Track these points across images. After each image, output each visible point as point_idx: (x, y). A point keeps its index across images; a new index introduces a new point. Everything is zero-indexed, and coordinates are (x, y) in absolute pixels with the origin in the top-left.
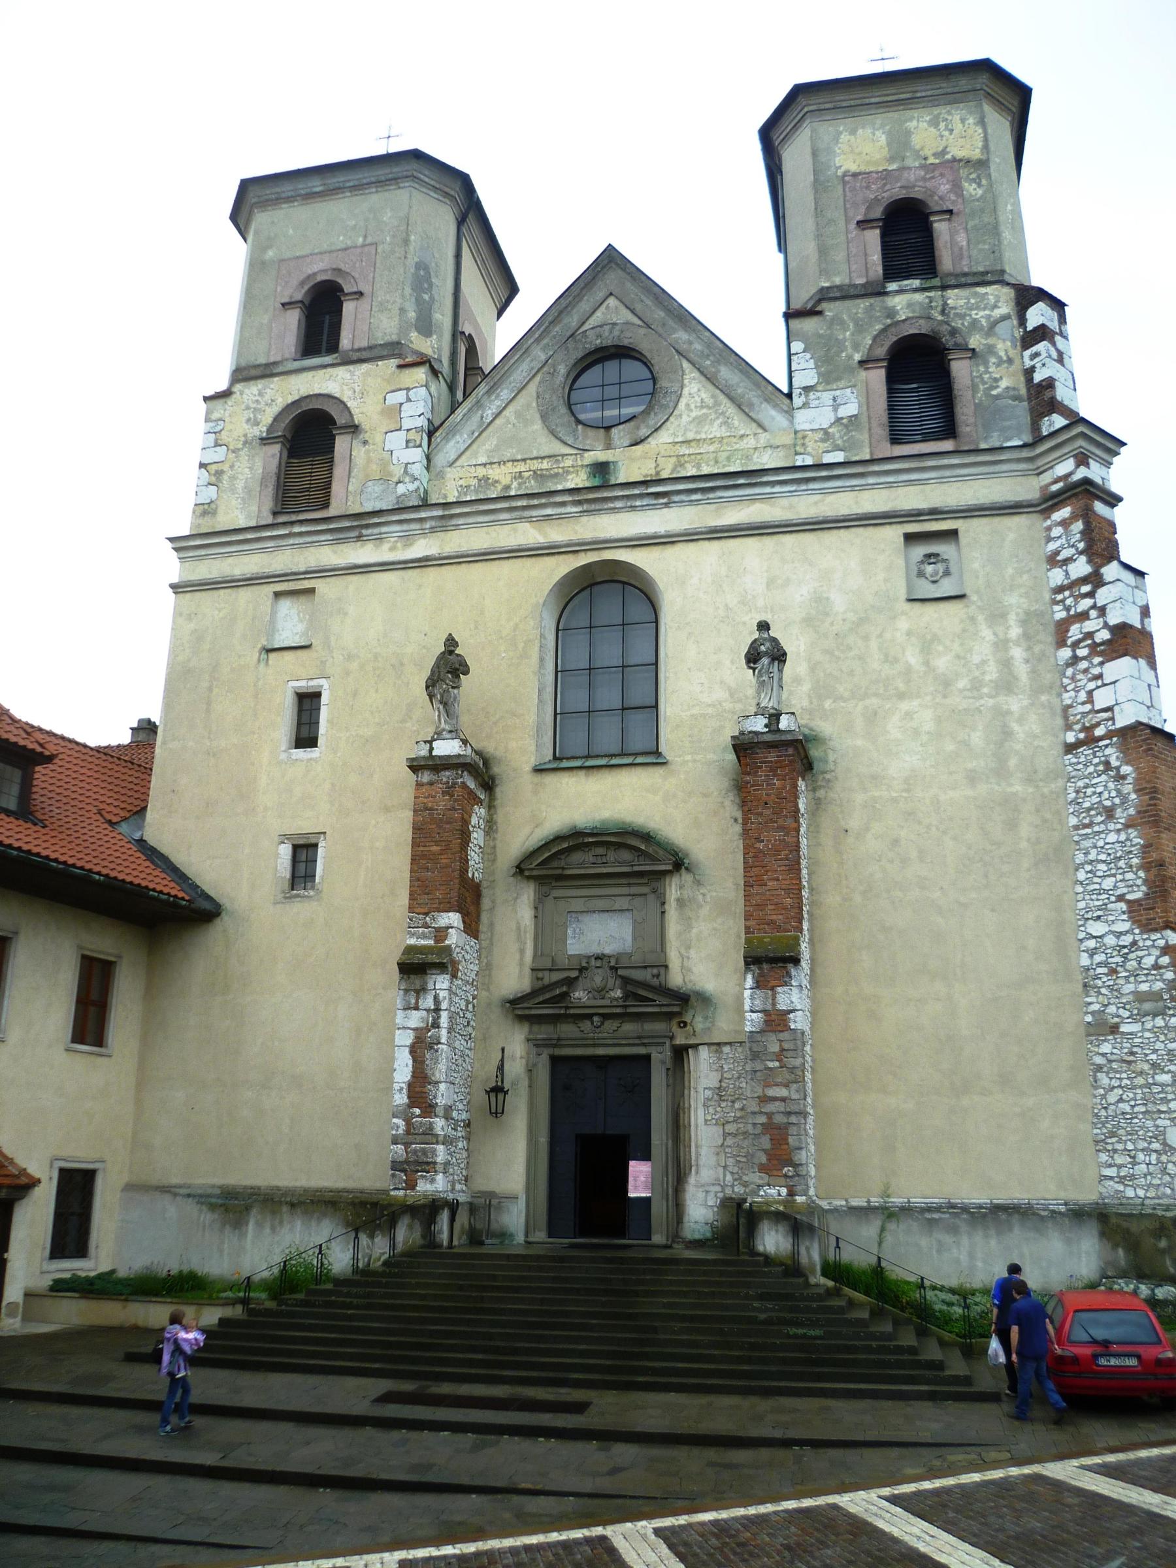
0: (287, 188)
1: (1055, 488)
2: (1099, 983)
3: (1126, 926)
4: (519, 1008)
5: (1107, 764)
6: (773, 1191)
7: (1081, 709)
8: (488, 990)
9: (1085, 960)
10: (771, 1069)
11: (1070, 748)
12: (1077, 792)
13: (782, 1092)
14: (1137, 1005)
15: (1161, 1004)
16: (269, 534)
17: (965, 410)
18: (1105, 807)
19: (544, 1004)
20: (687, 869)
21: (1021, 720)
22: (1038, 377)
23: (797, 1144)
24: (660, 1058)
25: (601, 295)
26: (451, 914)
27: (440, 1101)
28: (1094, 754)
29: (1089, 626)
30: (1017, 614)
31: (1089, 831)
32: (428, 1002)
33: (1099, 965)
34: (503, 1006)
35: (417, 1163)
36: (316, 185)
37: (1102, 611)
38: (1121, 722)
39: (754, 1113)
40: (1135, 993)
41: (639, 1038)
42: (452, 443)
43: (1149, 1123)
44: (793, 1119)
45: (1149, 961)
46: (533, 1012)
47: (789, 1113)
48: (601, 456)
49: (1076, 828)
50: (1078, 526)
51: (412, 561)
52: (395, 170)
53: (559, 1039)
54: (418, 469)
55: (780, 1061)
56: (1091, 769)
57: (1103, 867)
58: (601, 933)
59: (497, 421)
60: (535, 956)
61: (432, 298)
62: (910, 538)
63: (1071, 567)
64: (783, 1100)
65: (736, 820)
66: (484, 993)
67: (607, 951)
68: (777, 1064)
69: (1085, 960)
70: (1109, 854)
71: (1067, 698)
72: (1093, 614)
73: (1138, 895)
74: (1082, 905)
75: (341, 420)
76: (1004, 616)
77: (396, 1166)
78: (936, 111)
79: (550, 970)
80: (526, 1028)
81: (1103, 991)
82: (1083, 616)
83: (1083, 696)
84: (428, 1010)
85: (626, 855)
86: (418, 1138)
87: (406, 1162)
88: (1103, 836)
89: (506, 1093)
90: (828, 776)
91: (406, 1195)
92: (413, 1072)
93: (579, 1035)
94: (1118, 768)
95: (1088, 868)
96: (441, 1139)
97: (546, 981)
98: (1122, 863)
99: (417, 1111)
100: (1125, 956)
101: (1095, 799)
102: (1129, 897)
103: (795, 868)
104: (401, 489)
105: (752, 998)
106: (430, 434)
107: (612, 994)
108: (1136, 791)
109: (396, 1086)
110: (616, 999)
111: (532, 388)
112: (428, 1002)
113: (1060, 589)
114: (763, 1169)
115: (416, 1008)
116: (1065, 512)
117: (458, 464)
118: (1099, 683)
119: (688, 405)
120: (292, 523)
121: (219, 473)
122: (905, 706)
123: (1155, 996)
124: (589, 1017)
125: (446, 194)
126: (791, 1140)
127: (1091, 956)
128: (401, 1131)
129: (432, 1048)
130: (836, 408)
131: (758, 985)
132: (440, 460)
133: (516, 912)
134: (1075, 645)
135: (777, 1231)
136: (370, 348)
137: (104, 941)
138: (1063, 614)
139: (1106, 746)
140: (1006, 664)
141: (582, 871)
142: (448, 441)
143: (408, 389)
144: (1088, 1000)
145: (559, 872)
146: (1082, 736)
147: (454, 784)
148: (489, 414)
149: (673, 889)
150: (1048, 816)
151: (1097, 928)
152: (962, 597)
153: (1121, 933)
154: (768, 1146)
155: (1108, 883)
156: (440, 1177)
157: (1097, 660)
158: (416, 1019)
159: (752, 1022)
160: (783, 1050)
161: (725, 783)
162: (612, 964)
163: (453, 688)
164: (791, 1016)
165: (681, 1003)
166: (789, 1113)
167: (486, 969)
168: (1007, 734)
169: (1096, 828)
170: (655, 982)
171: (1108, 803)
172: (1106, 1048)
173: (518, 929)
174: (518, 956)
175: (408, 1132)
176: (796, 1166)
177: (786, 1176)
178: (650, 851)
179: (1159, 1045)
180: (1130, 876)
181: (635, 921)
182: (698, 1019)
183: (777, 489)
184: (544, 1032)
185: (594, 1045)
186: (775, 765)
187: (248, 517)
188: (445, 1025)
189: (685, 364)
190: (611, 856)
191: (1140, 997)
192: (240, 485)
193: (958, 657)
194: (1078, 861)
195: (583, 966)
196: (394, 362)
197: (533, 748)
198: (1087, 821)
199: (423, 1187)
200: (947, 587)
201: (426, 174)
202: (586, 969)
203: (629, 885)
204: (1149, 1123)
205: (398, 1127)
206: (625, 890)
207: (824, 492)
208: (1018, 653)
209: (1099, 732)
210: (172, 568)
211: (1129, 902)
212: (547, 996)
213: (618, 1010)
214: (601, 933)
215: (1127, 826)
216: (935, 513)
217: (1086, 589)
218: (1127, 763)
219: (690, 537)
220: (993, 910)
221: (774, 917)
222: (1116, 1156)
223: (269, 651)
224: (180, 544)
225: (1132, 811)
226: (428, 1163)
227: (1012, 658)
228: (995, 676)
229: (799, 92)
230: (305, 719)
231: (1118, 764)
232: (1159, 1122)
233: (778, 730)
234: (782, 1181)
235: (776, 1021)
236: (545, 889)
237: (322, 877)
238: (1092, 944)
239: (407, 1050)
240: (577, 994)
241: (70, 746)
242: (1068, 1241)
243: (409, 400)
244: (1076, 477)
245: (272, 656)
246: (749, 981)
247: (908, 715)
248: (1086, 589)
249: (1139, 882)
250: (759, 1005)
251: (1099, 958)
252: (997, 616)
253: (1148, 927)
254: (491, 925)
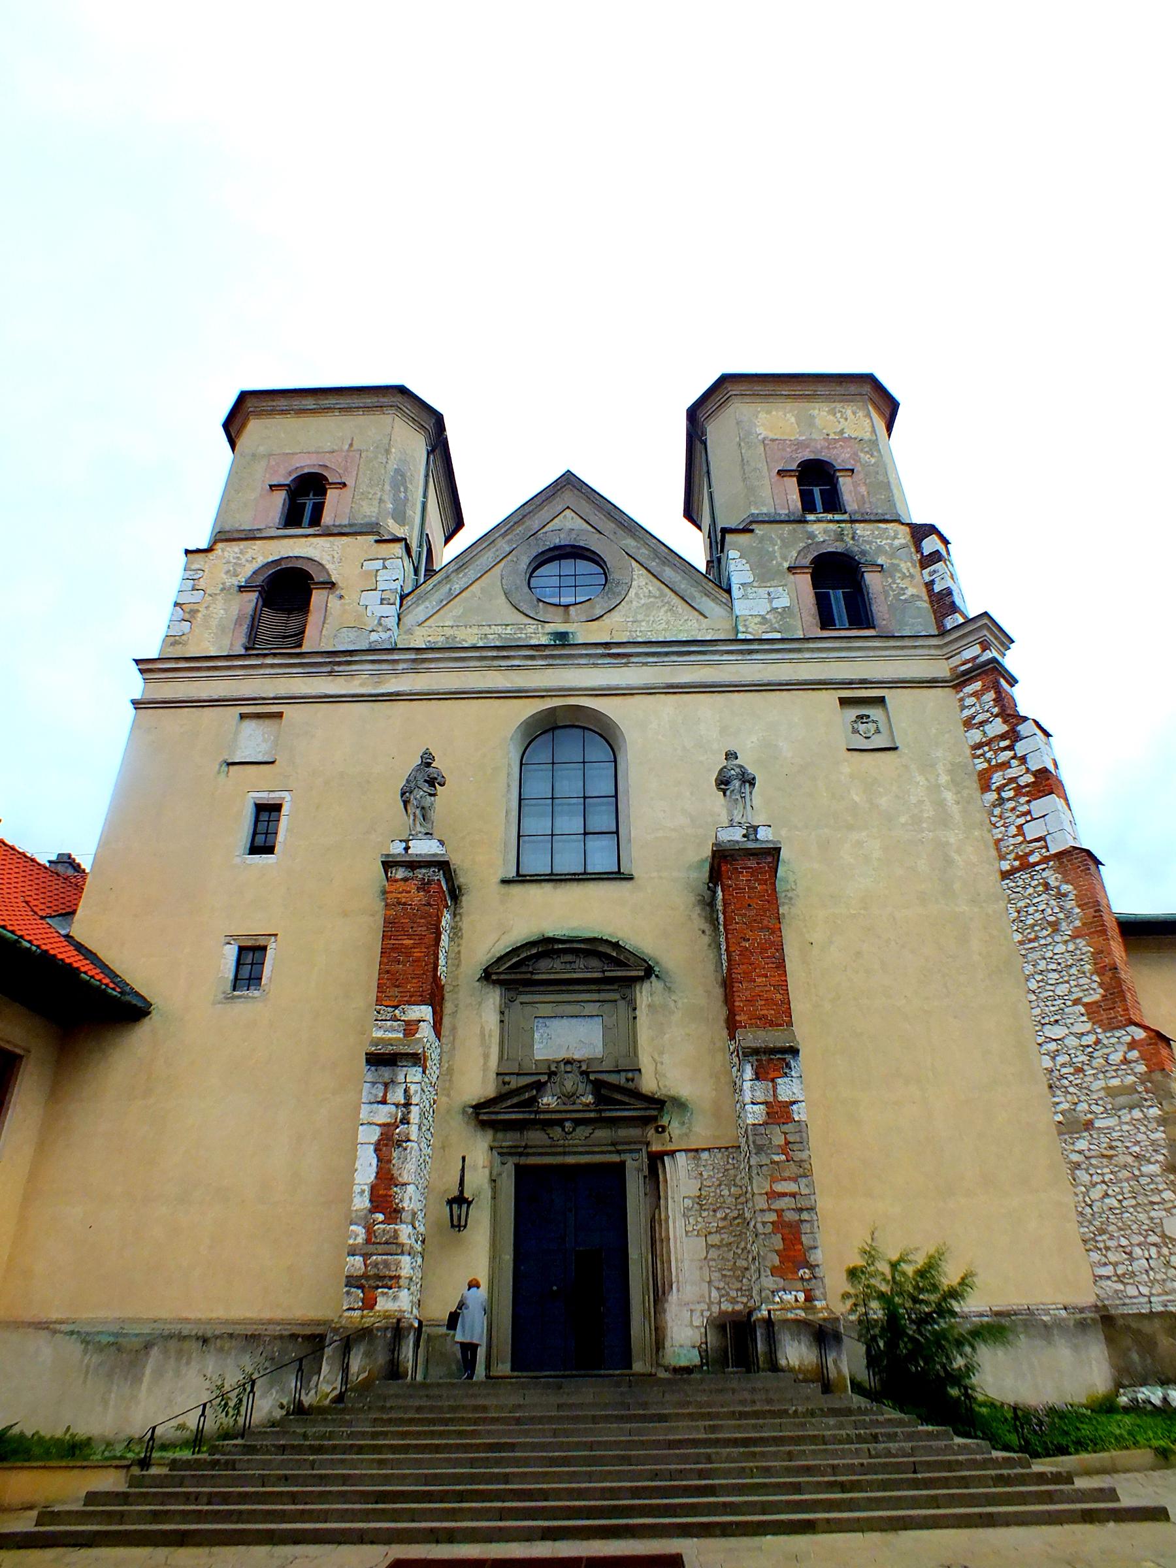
0: (282, 403)
1: (963, 668)
2: (1066, 1082)
3: (1088, 1026)
4: (483, 1115)
5: (1047, 886)
6: (789, 1297)
7: (1012, 841)
8: (448, 1096)
9: (1047, 1062)
10: (777, 1163)
11: (1005, 875)
12: (1019, 912)
13: (791, 1187)
14: (1109, 1099)
15: (1136, 1096)
16: (241, 663)
17: (881, 609)
18: (1049, 923)
19: (507, 1112)
20: (657, 976)
21: (959, 851)
22: (937, 588)
23: (812, 1244)
24: (634, 1167)
25: (560, 508)
26: (423, 1007)
28: (1032, 878)
29: (1011, 773)
30: (944, 765)
31: (1036, 944)
32: (398, 1096)
33: (1063, 1065)
34: (464, 1112)
35: (379, 1277)
36: (309, 403)
37: (1023, 760)
38: (1053, 851)
39: (762, 1211)
40: (1107, 1089)
41: (613, 1144)
42: (421, 608)
43: (1142, 1217)
44: (805, 1216)
45: (1116, 1057)
46: (501, 1117)
47: (801, 1210)
48: (562, 628)
49: (1021, 943)
50: (992, 695)
51: (383, 695)
52: (382, 400)
53: (526, 1147)
54: (392, 622)
55: (786, 1154)
56: (1031, 890)
57: (1055, 975)
58: (569, 1036)
59: (463, 594)
60: (501, 1058)
61: (406, 498)
62: (844, 702)
63: (987, 728)
64: (793, 1195)
65: (703, 932)
66: (444, 1099)
67: (576, 1057)
68: (783, 1157)
69: (1047, 1062)
70: (1059, 964)
71: (997, 834)
72: (1014, 763)
73: (1097, 997)
74: (1037, 1011)
75: (319, 577)
76: (933, 766)
77: (352, 1282)
78: (833, 405)
79: (518, 1074)
80: (489, 1135)
81: (1071, 1090)
82: (1006, 765)
83: (1013, 830)
84: (397, 1105)
85: (594, 963)
86: (380, 1248)
87: (365, 1276)
88: (1050, 948)
89: (469, 1203)
90: (789, 894)
91: (362, 1317)
92: (377, 1173)
93: (549, 1142)
94: (1058, 888)
95: (1039, 978)
96: (407, 1248)
97: (513, 1085)
98: (1074, 971)
99: (380, 1217)
100: (1090, 1055)
101: (1038, 916)
102: (1086, 1000)
103: (781, 965)
104: (374, 637)
105: (752, 1089)
106: (403, 598)
107: (583, 1099)
108: (1079, 906)
109: (357, 1189)
110: (587, 1105)
111: (497, 570)
112: (398, 1096)
113: (979, 746)
114: (774, 1271)
115: (384, 1102)
116: (977, 686)
117: (426, 624)
118: (1029, 818)
119: (637, 594)
120: (265, 655)
121: (194, 612)
122: (854, 836)
123: (1132, 1090)
124: (560, 1123)
126: (804, 1239)
127: (1053, 1058)
128: (360, 1240)
129: (399, 1146)
130: (771, 601)
131: (757, 1077)
132: (408, 620)
133: (481, 1017)
134: (999, 790)
135: (799, 1342)
136: (351, 525)
138: (986, 765)
139: (1043, 870)
140: (940, 804)
141: (552, 977)
142: (418, 605)
143: (384, 559)
144: (1057, 1100)
145: (529, 976)
146: (1017, 863)
147: (429, 882)
148: (457, 588)
149: (644, 995)
150: (995, 933)
151: (1058, 1032)
153: (1083, 1034)
154: (780, 1245)
155: (1062, 990)
156: (404, 1294)
157: (1023, 800)
158: (384, 1114)
159: (755, 1114)
160: (787, 1143)
161: (692, 899)
162: (584, 1068)
163: (431, 795)
164: (795, 1107)
165: (655, 1109)
166: (801, 1210)
167: (448, 1074)
168: (949, 862)
169: (1043, 942)
170: (631, 1085)
171: (1052, 919)
172: (1082, 1145)
173: (482, 1034)
174: (482, 1061)
175: (368, 1241)
176: (812, 1267)
177: (802, 1278)
178: (622, 958)
179: (1140, 1137)
180: (1082, 981)
181: (605, 1028)
182: (675, 1124)
183: (725, 657)
184: (509, 1139)
185: (565, 1154)
186: (741, 880)
187: (220, 648)
188: (417, 1121)
189: (634, 564)
190: (581, 963)
191: (1111, 1092)
192: (214, 623)
193: (897, 797)
194: (1027, 973)
195: (552, 1072)
197: (501, 862)
198: (1032, 936)
199: (384, 1304)
200: (879, 741)
201: (408, 407)
202: (555, 1073)
203: (599, 991)
204: (1142, 1217)
205: (357, 1235)
206: (595, 996)
207: (763, 662)
208: (949, 796)
209: (1033, 859)
210: (136, 686)
211: (1085, 1005)
212: (515, 1100)
213: (592, 1115)
214: (569, 1036)
215: (1073, 938)
216: (864, 683)
217: (1003, 744)
218: (1067, 883)
219: (649, 691)
220: (955, 1017)
221: (765, 1012)
222: (1109, 1254)
224: (145, 666)
225: (1078, 923)
226: (391, 1278)
227: (945, 799)
228: (932, 813)
229: (693, 414)
230: (262, 827)
231: (1057, 884)
232: (1153, 1214)
233: (757, 840)
234: (799, 1285)
235: (779, 1112)
236: (511, 994)
237: (270, 979)
238: (1053, 1046)
239: (372, 1147)
240: (545, 1100)
242: (1076, 1348)
243: (385, 567)
244: (982, 659)
245: (232, 768)
246: (749, 1073)
247: (859, 844)
248: (1003, 744)
249: (1095, 985)
250: (760, 1096)
251: (1061, 1059)
252: (927, 766)
253: (1111, 1027)
254: (454, 1029)
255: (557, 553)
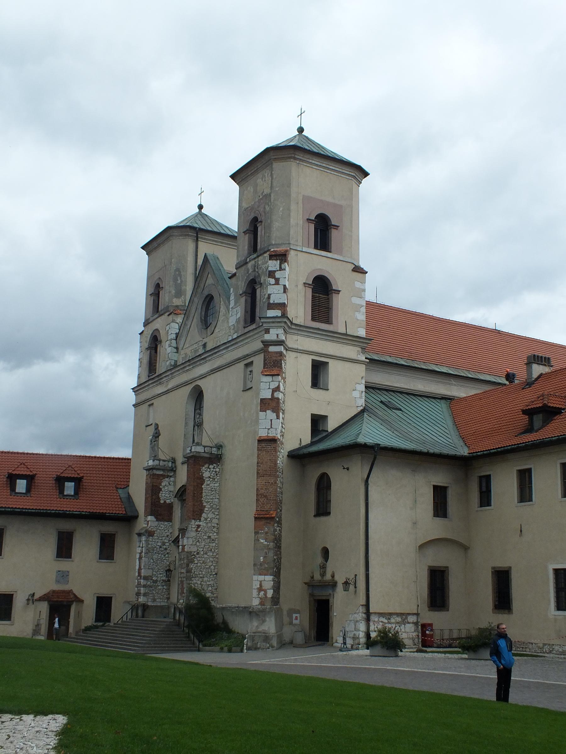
27: (142, 575)
36: (155, 244)
48: (205, 340)
61: (182, 281)
64: (183, 573)
112: (141, 545)
125: (186, 235)
132: (180, 349)
137: (109, 528)
148: (189, 326)
152: (252, 387)
158: (139, 550)
196: (167, 314)
201: (176, 232)
223: (147, 426)
241: (124, 461)
255: (209, 298)
